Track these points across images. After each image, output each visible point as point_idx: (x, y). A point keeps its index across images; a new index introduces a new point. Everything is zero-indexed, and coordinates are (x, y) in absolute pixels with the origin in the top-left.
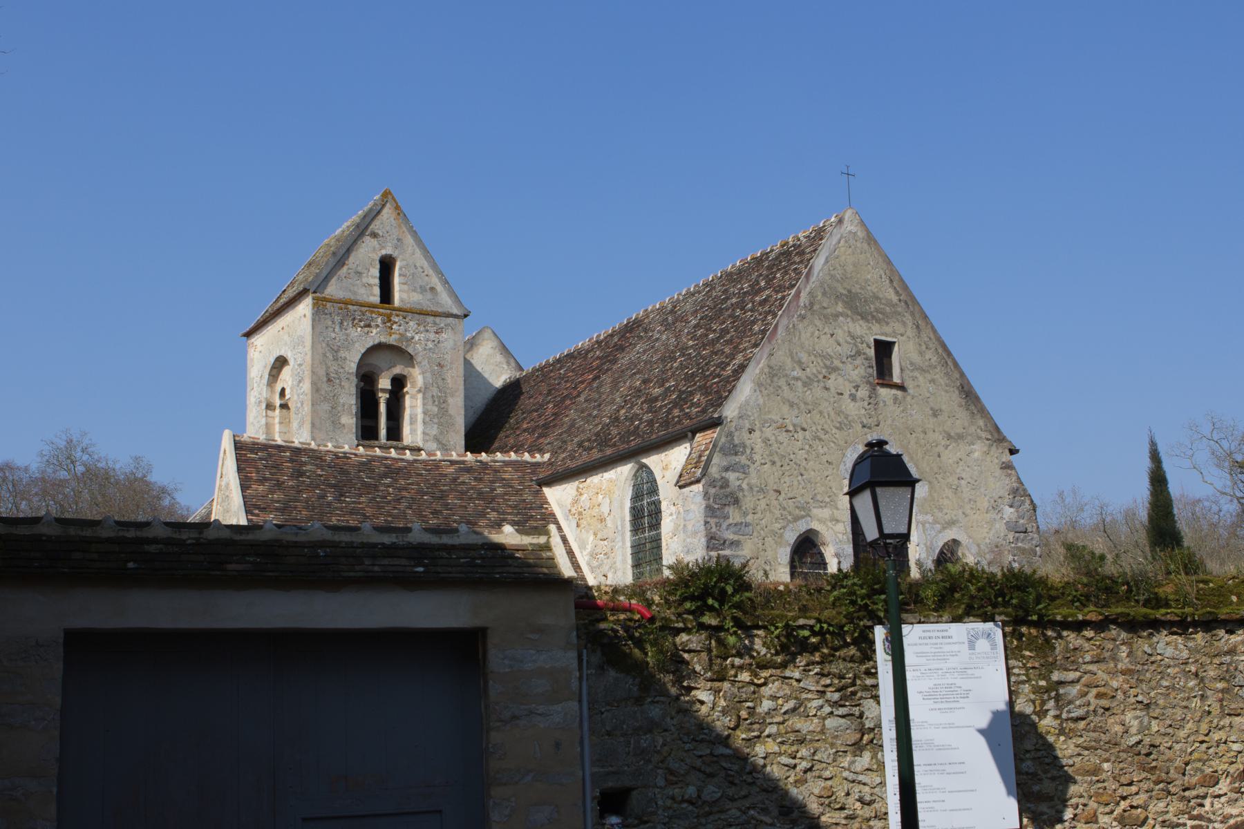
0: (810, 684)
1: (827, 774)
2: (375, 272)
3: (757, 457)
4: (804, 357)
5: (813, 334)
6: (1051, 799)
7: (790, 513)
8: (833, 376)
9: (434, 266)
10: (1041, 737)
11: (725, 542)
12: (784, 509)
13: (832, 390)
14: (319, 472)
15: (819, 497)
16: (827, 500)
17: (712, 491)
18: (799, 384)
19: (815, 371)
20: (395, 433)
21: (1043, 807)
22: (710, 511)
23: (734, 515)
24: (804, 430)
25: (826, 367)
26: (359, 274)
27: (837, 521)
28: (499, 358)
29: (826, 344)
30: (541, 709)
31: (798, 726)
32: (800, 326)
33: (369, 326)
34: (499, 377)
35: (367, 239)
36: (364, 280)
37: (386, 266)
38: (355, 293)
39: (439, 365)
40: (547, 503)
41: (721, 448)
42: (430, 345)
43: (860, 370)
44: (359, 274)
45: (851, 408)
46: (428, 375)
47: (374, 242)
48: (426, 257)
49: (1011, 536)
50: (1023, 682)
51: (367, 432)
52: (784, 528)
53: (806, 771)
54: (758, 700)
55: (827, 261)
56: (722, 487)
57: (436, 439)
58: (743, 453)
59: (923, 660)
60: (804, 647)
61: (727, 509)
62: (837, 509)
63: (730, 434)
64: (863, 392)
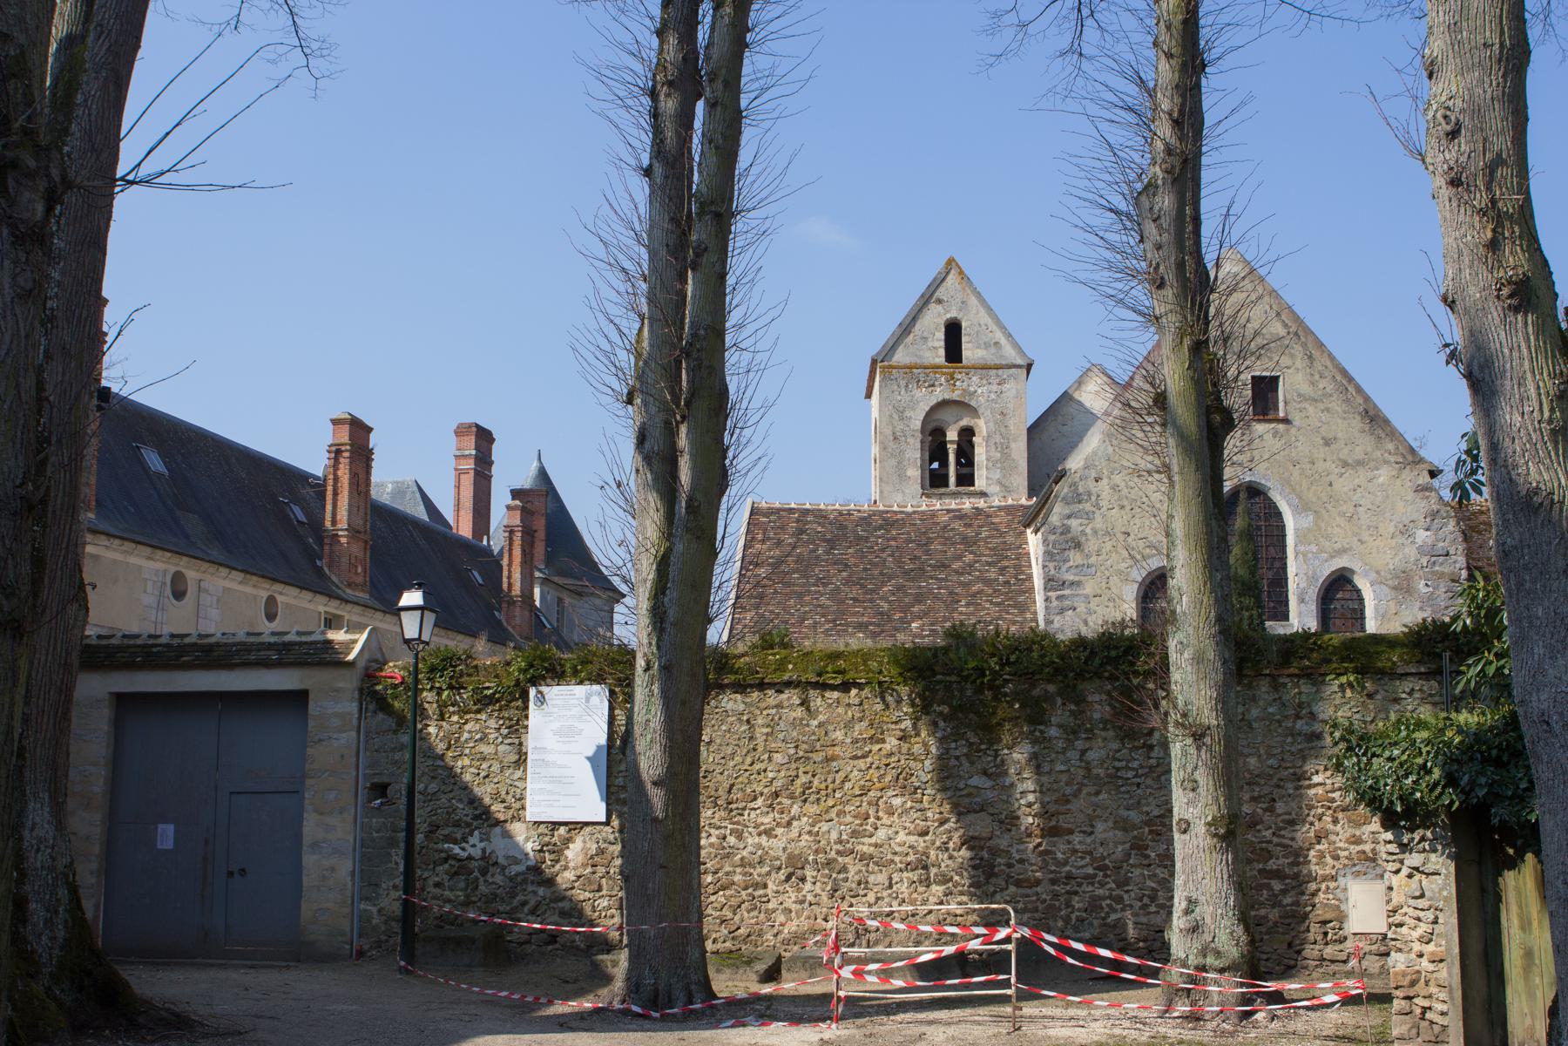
0: (492, 723)
1: (496, 780)
2: (941, 335)
9: (998, 322)
11: (1064, 583)
14: (819, 529)
17: (1052, 538)
20: (966, 479)
23: (1075, 558)
26: (925, 339)
30: (335, 736)
31: (482, 750)
33: (933, 385)
36: (930, 344)
37: (953, 332)
38: (920, 357)
40: (1027, 543)
41: (1063, 499)
42: (993, 396)
44: (925, 339)
47: (939, 308)
51: (936, 481)
53: (485, 778)
56: (1062, 533)
57: (1000, 483)
58: (1087, 501)
60: (491, 700)
61: (1067, 552)
63: (1074, 484)
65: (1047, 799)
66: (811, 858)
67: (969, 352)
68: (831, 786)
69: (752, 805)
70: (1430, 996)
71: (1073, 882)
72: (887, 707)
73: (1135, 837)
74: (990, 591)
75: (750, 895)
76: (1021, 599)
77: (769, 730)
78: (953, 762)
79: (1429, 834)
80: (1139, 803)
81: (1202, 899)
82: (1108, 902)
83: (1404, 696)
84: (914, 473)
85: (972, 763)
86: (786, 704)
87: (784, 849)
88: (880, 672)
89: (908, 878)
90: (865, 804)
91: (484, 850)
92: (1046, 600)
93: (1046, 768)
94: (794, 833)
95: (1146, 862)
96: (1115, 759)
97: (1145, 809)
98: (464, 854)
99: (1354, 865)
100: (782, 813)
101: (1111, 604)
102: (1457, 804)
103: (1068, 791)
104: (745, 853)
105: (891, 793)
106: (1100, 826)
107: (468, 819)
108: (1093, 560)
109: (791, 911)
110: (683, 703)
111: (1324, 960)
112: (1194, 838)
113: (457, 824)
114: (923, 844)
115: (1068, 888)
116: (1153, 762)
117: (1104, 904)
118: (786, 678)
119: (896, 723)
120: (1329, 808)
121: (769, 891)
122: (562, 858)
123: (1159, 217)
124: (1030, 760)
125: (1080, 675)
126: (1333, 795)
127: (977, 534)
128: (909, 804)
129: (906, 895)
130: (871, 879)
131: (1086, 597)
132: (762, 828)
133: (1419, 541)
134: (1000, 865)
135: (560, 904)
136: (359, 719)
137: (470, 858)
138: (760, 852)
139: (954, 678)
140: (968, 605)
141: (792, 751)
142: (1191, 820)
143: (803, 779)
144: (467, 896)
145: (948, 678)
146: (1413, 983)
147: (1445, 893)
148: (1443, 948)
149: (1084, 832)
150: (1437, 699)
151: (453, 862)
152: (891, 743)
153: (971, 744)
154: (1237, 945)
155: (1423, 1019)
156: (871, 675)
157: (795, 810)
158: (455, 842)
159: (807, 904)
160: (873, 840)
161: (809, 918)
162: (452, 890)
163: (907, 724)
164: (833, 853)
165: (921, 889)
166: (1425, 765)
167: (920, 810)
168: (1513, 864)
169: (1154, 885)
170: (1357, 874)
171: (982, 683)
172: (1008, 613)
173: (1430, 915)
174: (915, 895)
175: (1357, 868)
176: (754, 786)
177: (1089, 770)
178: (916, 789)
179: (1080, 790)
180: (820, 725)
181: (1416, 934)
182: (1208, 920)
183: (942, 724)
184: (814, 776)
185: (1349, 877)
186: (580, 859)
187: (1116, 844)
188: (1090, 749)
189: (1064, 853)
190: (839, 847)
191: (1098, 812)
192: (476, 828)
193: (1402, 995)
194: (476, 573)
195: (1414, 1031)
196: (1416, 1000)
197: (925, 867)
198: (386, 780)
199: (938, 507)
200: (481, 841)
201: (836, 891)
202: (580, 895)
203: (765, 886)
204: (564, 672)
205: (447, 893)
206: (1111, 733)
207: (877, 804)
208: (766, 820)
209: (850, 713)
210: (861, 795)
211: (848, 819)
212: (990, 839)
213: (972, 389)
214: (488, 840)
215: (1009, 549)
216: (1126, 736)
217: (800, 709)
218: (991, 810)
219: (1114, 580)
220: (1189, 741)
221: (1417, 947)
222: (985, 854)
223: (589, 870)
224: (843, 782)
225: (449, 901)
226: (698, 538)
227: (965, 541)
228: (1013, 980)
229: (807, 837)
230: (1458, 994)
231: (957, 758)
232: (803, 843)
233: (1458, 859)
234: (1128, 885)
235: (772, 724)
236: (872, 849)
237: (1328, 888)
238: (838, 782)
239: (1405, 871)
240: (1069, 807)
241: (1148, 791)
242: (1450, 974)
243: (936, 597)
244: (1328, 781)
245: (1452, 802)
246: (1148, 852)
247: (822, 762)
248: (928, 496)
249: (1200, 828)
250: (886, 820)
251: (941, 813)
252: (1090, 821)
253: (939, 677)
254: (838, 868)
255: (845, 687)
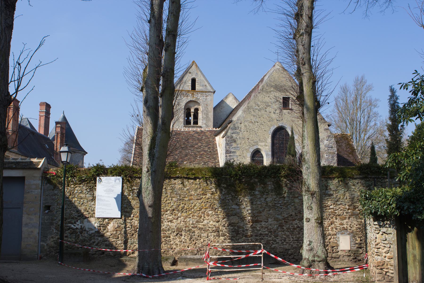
0: (84, 188)
1: (85, 205)
2: (190, 82)
3: (242, 130)
4: (259, 103)
5: (262, 97)
6: (129, 212)
7: (251, 144)
8: (268, 108)
9: (206, 79)
10: (128, 200)
11: (231, 152)
12: (250, 143)
13: (268, 111)
15: (261, 140)
16: (264, 140)
17: (228, 139)
18: (257, 110)
19: (262, 107)
20: (196, 123)
21: (127, 214)
22: (227, 144)
23: (234, 145)
24: (258, 122)
25: (266, 105)
27: (267, 146)
28: (234, 101)
29: (267, 99)
30: (34, 191)
31: (81, 196)
32: (259, 95)
33: (188, 96)
34: (234, 106)
35: (188, 74)
36: (187, 85)
37: (194, 81)
39: (207, 105)
40: (216, 141)
41: (231, 128)
42: (204, 100)
43: (277, 106)
45: (273, 116)
46: (203, 108)
47: (190, 74)
48: (204, 77)
49: (326, 149)
50: (126, 189)
51: (188, 123)
52: (249, 148)
53: (82, 204)
54: (74, 191)
55: (269, 77)
56: (231, 138)
57: (205, 124)
58: (238, 129)
59: (105, 184)
60: (84, 181)
61: (232, 143)
62: (267, 142)
63: (234, 124)
64: (278, 111)
65: (255, 212)
66: (184, 229)
67: (198, 87)
68: (190, 208)
69: (166, 213)
70: (388, 268)
71: (262, 236)
72: (208, 185)
73: (280, 223)
74: (206, 154)
75: (165, 240)
76: (215, 156)
77: (171, 191)
78: (227, 201)
79: (388, 222)
80: (281, 213)
81: (314, 241)
82: (272, 241)
83: (356, 184)
84: (182, 120)
85: (233, 201)
86: (177, 183)
87: (176, 226)
88: (206, 175)
89: (213, 235)
90: (200, 213)
91: (81, 226)
92: (226, 156)
93: (255, 203)
94: (179, 221)
95: (283, 230)
96: (274, 201)
97: (283, 215)
98: (75, 227)
99: (341, 231)
100: (175, 215)
101: (244, 158)
102: (399, 214)
103: (261, 210)
104: (164, 227)
105: (208, 210)
106: (270, 220)
107: (76, 217)
108: (239, 146)
109: (177, 244)
110: (159, 182)
111: (333, 257)
112: (311, 223)
113: (73, 218)
114: (218, 225)
115: (260, 237)
116: (285, 202)
117: (271, 242)
118: (177, 175)
119: (210, 189)
120: (335, 215)
121: (171, 239)
122: (106, 229)
123: (304, 45)
124: (250, 201)
125: (266, 177)
126: (336, 211)
127: (202, 138)
128: (214, 213)
129: (212, 240)
130: (202, 235)
131: (237, 156)
132: (169, 220)
133: (325, 143)
134: (240, 231)
135: (106, 243)
136: (42, 186)
137: (77, 228)
138: (168, 227)
139: (228, 177)
140: (200, 157)
141: (179, 197)
142: (310, 218)
143: (182, 205)
144: (76, 240)
145: (226, 177)
146: (383, 265)
147: (393, 239)
148: (392, 255)
149: (265, 222)
150: (365, 185)
151: (71, 230)
152: (209, 195)
153: (233, 196)
154: (324, 254)
155: (386, 275)
156: (203, 175)
157: (179, 215)
158: (72, 224)
159: (182, 242)
160: (203, 224)
161: (183, 246)
162: (70, 238)
163: (214, 190)
164: (191, 227)
165: (217, 238)
166: (390, 203)
167: (217, 215)
168: (410, 231)
169: (285, 237)
170: (342, 234)
171: (237, 178)
172: (211, 160)
173: (388, 246)
174: (215, 240)
175: (342, 232)
176: (167, 207)
177: (267, 204)
178: (216, 209)
179: (264, 210)
180: (187, 190)
181: (384, 251)
182: (315, 247)
183: (224, 190)
184: (185, 205)
185: (340, 234)
186: (112, 229)
187: (274, 225)
188: (268, 198)
189: (259, 228)
190: (193, 226)
191: (270, 216)
192: (79, 219)
193: (380, 268)
194: (46, 145)
195: (383, 278)
196: (384, 270)
197: (218, 232)
198: (50, 205)
199: (191, 130)
200: (80, 223)
201: (191, 238)
202: (112, 240)
203: (170, 237)
204: (107, 173)
205: (69, 239)
206: (274, 193)
207: (204, 213)
208: (170, 218)
209: (196, 186)
210: (199, 210)
211: (196, 217)
212: (238, 223)
213: (198, 98)
214: (83, 223)
215: (211, 142)
216: (278, 194)
217: (181, 185)
218: (238, 215)
219: (245, 151)
220: (310, 195)
221: (384, 254)
222: (236, 228)
223: (115, 232)
224: (194, 207)
225: (69, 241)
226: (166, 132)
227: (198, 139)
228: (262, 265)
229: (183, 223)
230: (397, 268)
231: (228, 200)
232: (181, 224)
233: (396, 229)
234: (278, 237)
235: (173, 189)
236: (202, 226)
237: (334, 237)
238: (192, 206)
239: (381, 233)
240: (261, 214)
241: (284, 210)
242: (394, 262)
243: (191, 155)
244: (335, 208)
245: (397, 214)
246: (284, 227)
247: (188, 201)
248: (185, 127)
249: (313, 221)
250: (207, 218)
251: (223, 216)
252: (267, 218)
253: (224, 176)
254: (192, 232)
255: (195, 179)
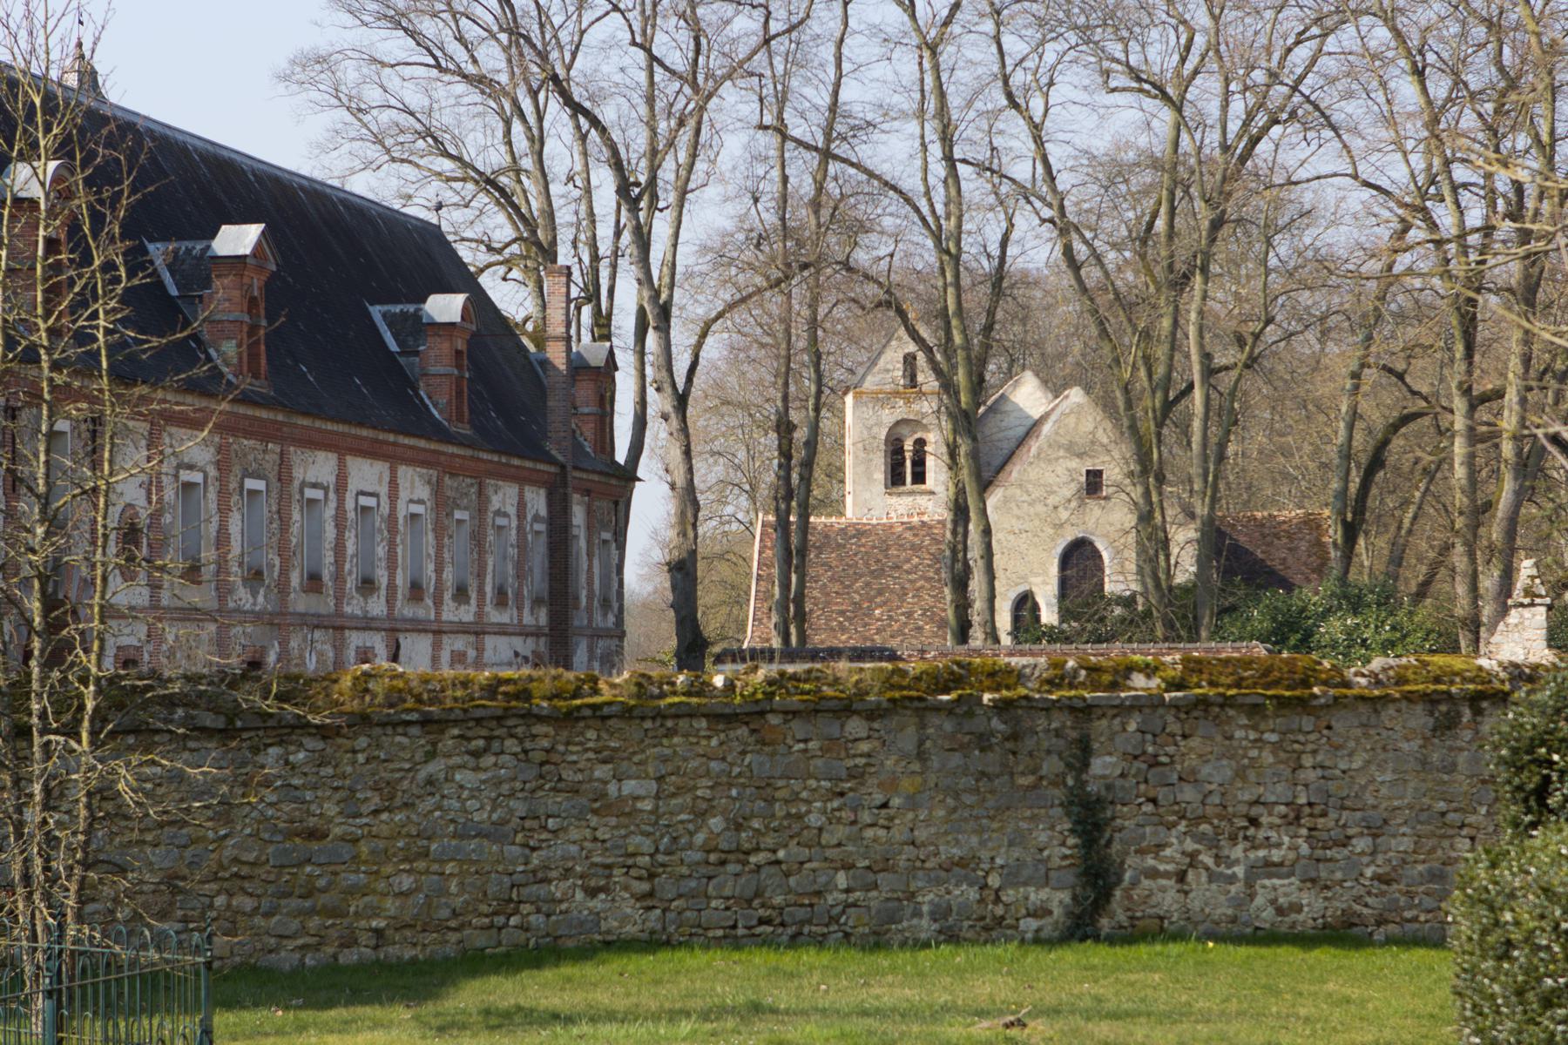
20: (919, 477)
29: (1050, 478)
227: (914, 548)
243: (892, 591)
